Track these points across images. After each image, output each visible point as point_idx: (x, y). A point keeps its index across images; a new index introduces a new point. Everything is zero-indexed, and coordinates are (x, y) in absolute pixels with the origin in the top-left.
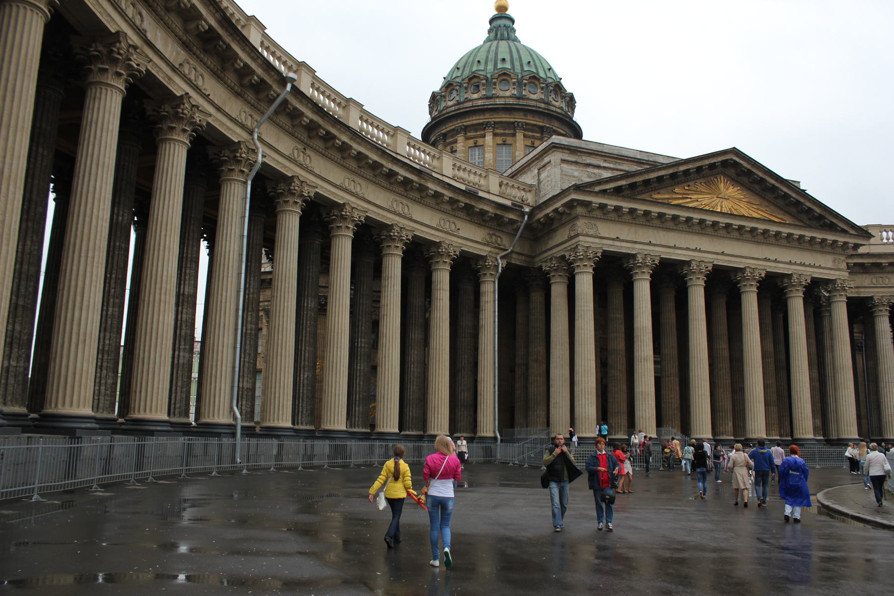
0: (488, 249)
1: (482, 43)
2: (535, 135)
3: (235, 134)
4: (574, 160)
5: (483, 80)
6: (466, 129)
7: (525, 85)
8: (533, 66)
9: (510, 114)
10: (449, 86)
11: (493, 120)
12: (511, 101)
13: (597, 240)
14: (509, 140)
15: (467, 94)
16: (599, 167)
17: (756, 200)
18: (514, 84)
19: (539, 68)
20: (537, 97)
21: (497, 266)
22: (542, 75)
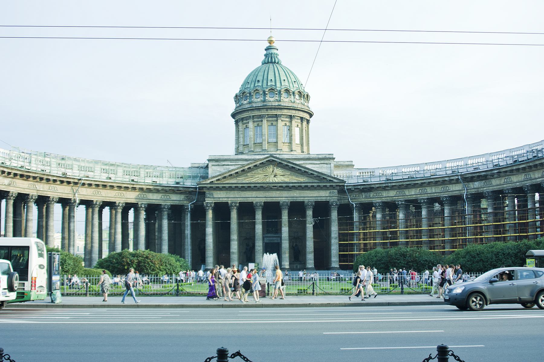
0: (185, 202)
1: (260, 64)
2: (274, 119)
3: (70, 196)
4: (217, 164)
5: (248, 94)
6: (242, 119)
7: (267, 94)
8: (274, 81)
9: (259, 111)
10: (236, 96)
11: (252, 115)
12: (260, 104)
13: (212, 199)
14: (260, 123)
15: (242, 101)
16: (228, 165)
17: (288, 173)
18: (261, 94)
19: (277, 81)
20: (274, 99)
21: (189, 208)
22: (278, 85)
